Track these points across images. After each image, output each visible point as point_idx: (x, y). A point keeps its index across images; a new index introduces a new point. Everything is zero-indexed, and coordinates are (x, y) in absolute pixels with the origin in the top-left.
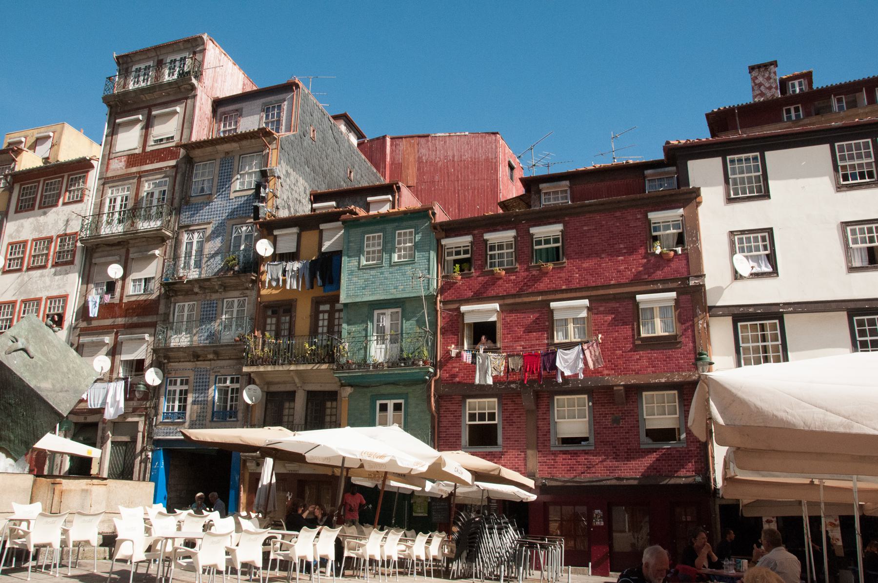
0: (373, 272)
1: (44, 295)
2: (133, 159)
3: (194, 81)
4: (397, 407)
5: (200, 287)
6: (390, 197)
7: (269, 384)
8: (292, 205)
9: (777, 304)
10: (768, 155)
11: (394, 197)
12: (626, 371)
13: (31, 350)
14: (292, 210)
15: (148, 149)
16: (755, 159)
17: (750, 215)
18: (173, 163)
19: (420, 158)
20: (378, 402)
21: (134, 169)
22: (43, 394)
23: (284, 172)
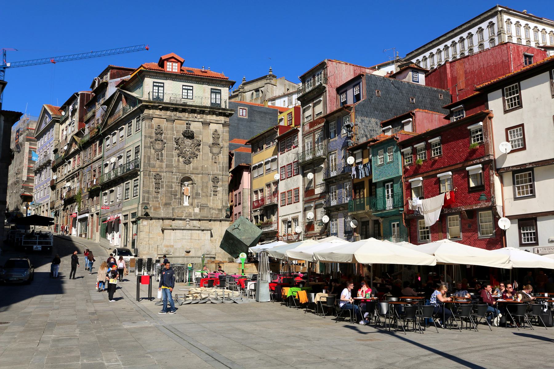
0: (382, 168)
1: (292, 188)
2: (312, 124)
3: (324, 85)
4: (398, 225)
5: (336, 180)
6: (411, 119)
7: (361, 218)
8: (368, 134)
9: (525, 164)
10: (521, 82)
11: (412, 118)
12: (465, 204)
13: (240, 228)
14: (369, 136)
15: (315, 119)
16: (516, 86)
17: (514, 119)
18: (323, 124)
19: (465, 71)
20: (392, 223)
21: (312, 129)
22: (242, 240)
23: (360, 120)
